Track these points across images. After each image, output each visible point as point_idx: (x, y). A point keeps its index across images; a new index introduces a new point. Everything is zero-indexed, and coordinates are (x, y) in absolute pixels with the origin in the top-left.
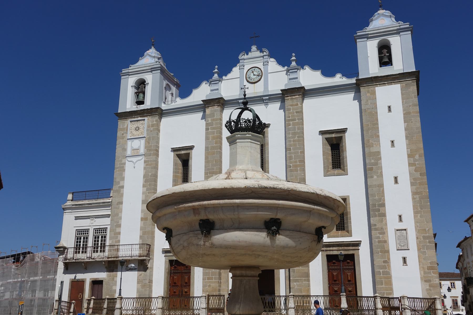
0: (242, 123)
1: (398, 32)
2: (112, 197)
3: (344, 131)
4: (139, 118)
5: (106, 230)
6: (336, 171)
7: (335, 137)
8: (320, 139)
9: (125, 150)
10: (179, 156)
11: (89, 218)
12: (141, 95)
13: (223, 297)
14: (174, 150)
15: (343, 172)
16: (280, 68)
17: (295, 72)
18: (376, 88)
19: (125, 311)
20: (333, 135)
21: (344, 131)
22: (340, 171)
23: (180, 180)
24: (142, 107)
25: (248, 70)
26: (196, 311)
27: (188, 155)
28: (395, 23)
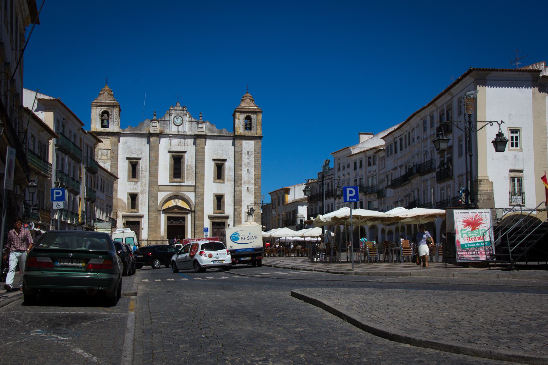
1: (255, 113)
3: (225, 160)
4: (106, 137)
6: (218, 181)
7: (220, 163)
8: (213, 163)
10: (130, 162)
12: (105, 121)
14: (128, 159)
15: (223, 181)
16: (193, 120)
17: (202, 124)
18: (243, 141)
20: (220, 162)
21: (225, 160)
22: (221, 181)
23: (131, 176)
24: (107, 130)
25: (175, 117)
27: (138, 162)
28: (254, 106)
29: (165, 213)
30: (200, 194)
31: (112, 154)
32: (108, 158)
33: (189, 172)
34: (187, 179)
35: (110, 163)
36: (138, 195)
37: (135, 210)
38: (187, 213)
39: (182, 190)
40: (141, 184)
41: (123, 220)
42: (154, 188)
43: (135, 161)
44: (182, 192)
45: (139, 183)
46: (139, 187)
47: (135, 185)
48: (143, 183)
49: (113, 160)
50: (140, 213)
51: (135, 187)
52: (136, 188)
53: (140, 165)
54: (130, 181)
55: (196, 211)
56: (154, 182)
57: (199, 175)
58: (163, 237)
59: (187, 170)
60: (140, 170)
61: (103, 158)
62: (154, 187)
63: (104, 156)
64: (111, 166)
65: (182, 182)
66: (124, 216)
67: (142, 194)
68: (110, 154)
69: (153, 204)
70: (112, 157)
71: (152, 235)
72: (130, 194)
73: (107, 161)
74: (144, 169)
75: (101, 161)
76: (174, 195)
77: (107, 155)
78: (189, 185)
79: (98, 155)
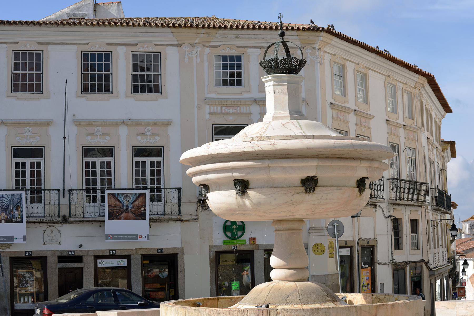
0: (293, 62)
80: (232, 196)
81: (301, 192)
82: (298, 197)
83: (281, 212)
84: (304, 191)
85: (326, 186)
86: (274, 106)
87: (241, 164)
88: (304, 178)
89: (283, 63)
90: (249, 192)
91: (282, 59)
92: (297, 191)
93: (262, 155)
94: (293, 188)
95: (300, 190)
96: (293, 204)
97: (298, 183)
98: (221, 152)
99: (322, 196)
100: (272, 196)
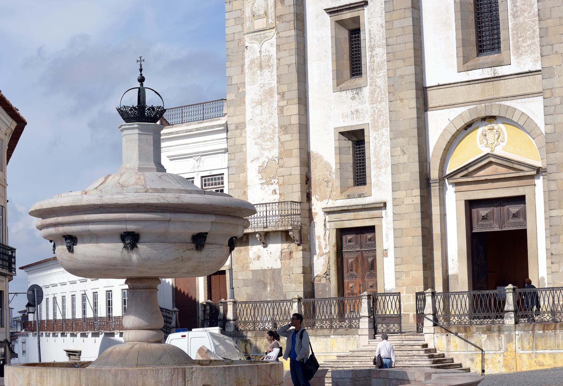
2: (226, 114)
5: (222, 178)
9: (240, 20)
10: (340, 23)
11: (191, 157)
13: (398, 296)
14: (331, 11)
19: (280, 323)
23: (347, 72)
26: (354, 321)
27: (356, 20)
29: (457, 184)
30: (558, 101)
31: (279, 6)
32: (270, 21)
33: (521, 19)
34: (517, 48)
35: (274, 40)
36: (366, 133)
37: (361, 189)
38: (532, 177)
39: (502, 95)
40: (372, 92)
41: (328, 225)
42: (402, 100)
43: (347, 15)
44: (501, 103)
45: (366, 91)
46: (367, 107)
47: (353, 98)
48: (378, 90)
49: (284, 24)
50: (374, 197)
51: (355, 105)
52: (357, 111)
53: (367, 26)
54: (341, 90)
55: (548, 171)
56: (402, 77)
57: (549, 22)
58: (456, 276)
59: (515, 16)
60: (368, 45)
61: (260, 24)
62: (402, 95)
63: (259, 17)
64: (278, 46)
65: (500, 64)
66: (329, 212)
67: (376, 129)
68: (273, 9)
69: (404, 159)
70: (278, 18)
71: (407, 273)
72: (342, 133)
73: (268, 33)
74: (377, 38)
75: (251, 39)
76: (475, 117)
77: (266, 13)
78: (527, 70)
79: (243, 19)
80: (117, 249)
81: (192, 249)
82: (189, 253)
83: (168, 268)
84: (195, 248)
85: (212, 244)
86: (138, 156)
87: (142, 216)
88: (195, 234)
89: (151, 111)
90: (138, 245)
91: (150, 107)
92: (189, 248)
93: (162, 208)
94: (185, 244)
95: (191, 246)
96: (182, 261)
97: (189, 239)
98: (120, 202)
99: (208, 254)
100: (164, 252)
